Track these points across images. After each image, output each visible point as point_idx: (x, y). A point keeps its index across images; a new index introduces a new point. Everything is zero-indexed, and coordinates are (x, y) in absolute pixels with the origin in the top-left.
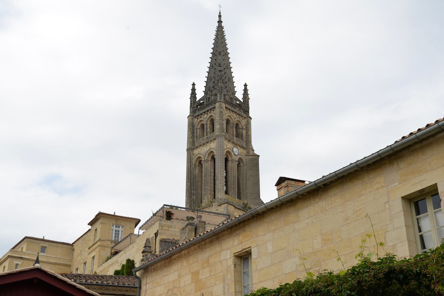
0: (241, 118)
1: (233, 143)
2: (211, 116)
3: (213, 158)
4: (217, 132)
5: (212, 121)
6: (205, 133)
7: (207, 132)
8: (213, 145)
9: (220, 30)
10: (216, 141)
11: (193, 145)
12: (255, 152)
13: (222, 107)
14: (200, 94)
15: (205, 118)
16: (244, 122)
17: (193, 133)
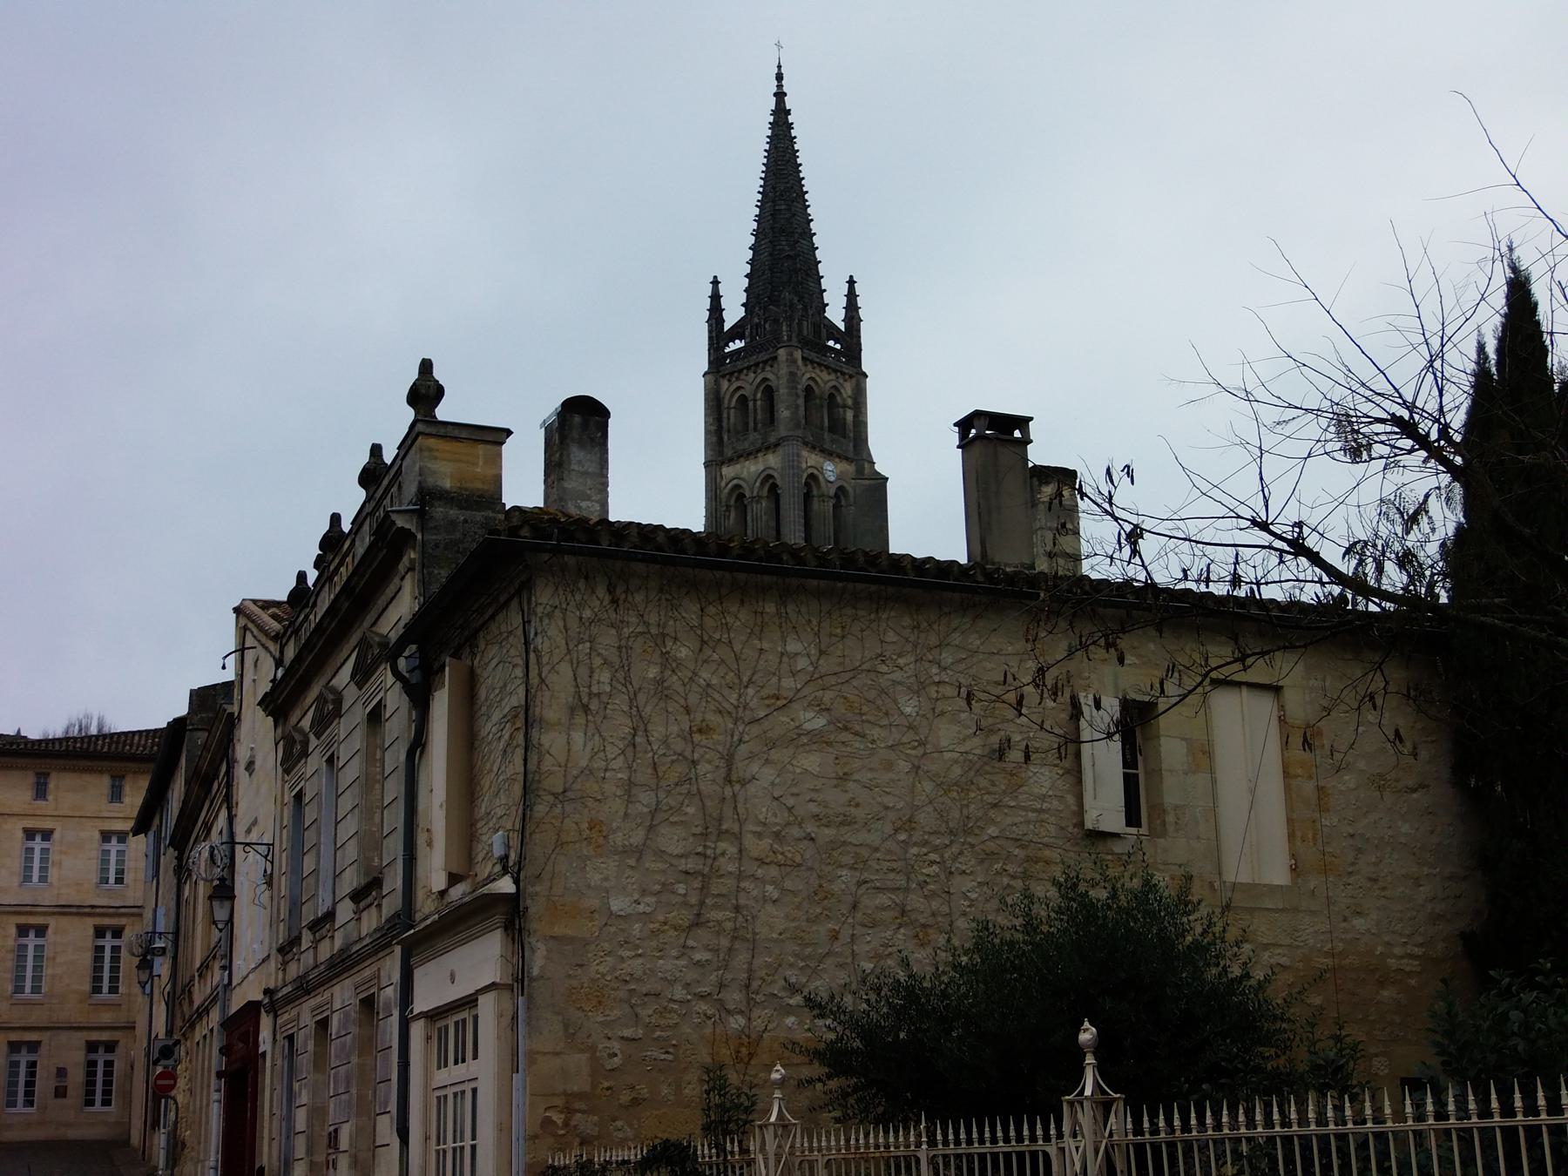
1: (823, 451)
2: (765, 379)
3: (774, 487)
4: (783, 431)
5: (769, 393)
6: (751, 425)
7: (755, 423)
8: (773, 460)
9: (781, 117)
10: (780, 451)
11: (721, 453)
12: (877, 467)
13: (794, 361)
14: (733, 313)
15: (749, 383)
16: (848, 389)
17: (719, 420)
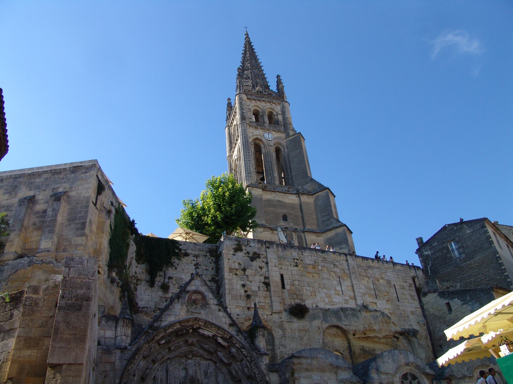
0: (274, 105)
16: (278, 109)
